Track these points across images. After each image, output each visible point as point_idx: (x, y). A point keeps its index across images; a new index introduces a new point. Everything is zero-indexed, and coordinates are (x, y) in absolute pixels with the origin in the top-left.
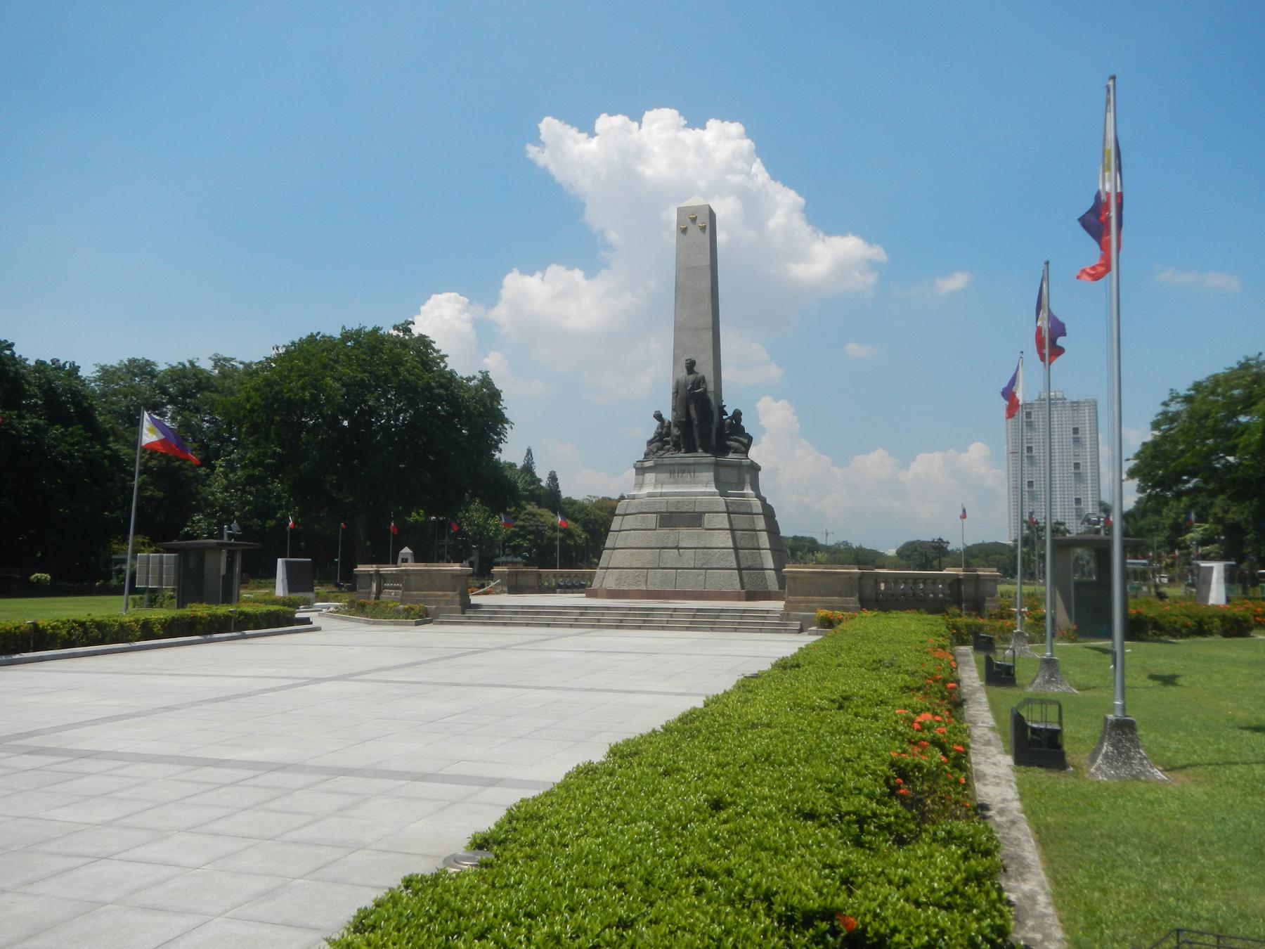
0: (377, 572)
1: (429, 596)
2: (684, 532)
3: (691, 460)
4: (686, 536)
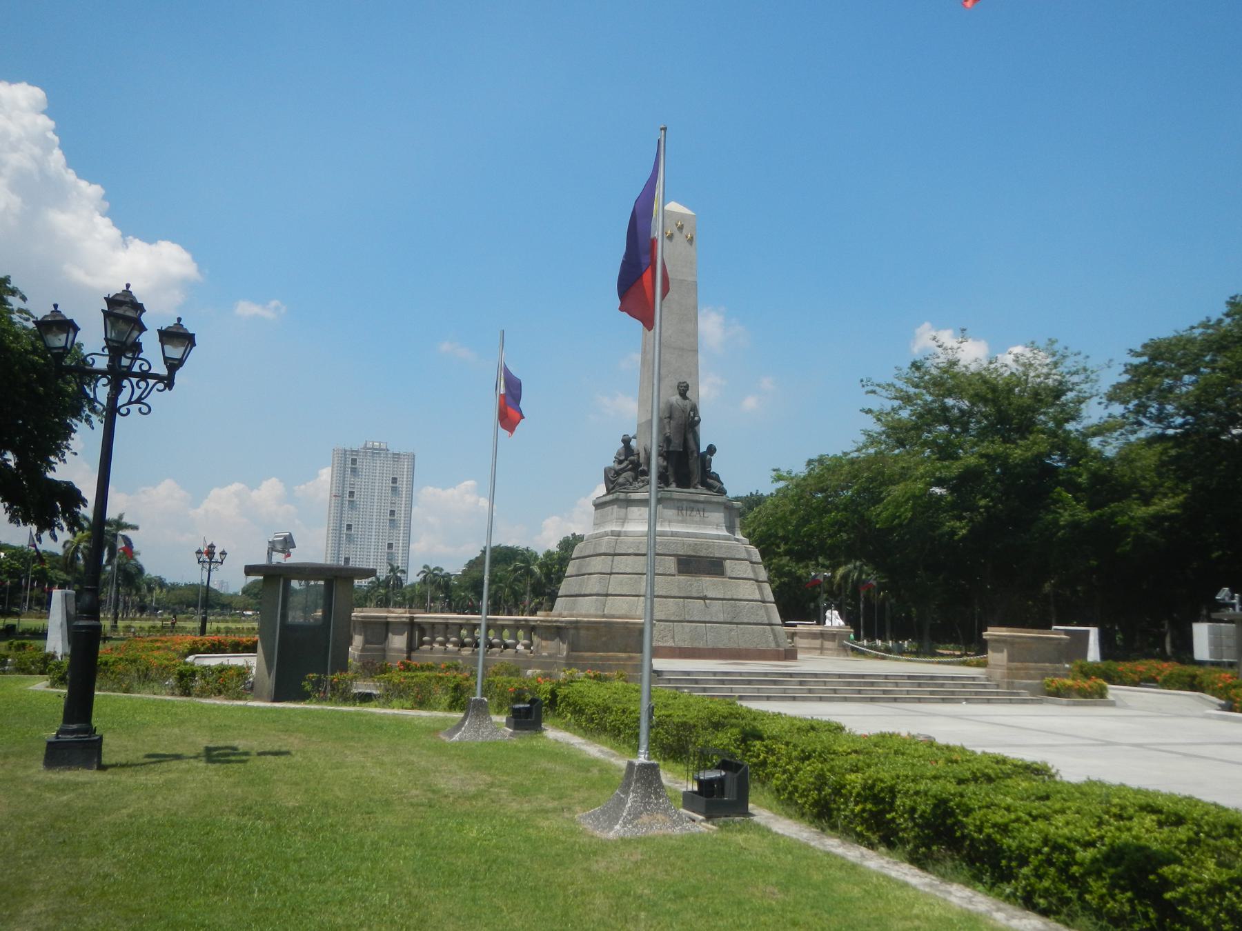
0: (412, 619)
1: (608, 659)
3: (702, 498)
4: (708, 585)
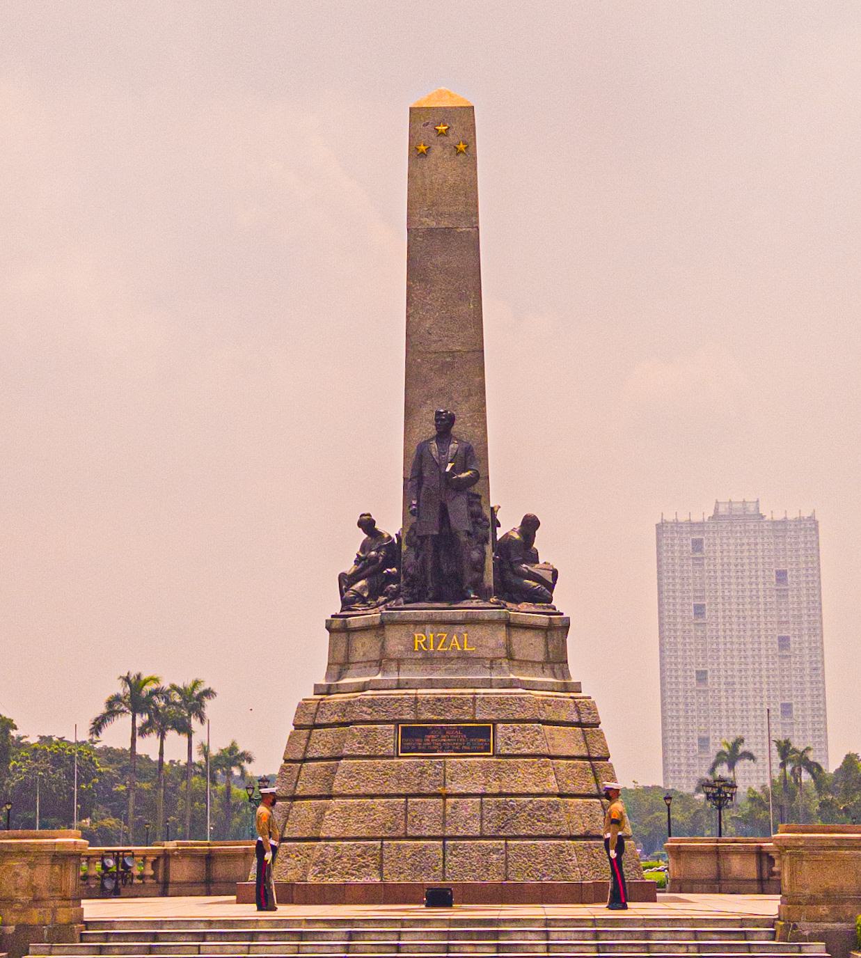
2: (455, 762)
3: (459, 614)
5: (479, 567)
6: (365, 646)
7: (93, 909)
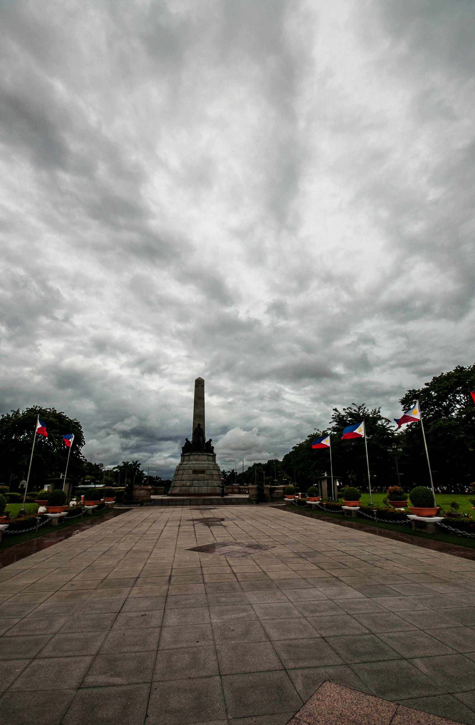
5: (203, 446)
6: (186, 458)
7: (153, 497)
